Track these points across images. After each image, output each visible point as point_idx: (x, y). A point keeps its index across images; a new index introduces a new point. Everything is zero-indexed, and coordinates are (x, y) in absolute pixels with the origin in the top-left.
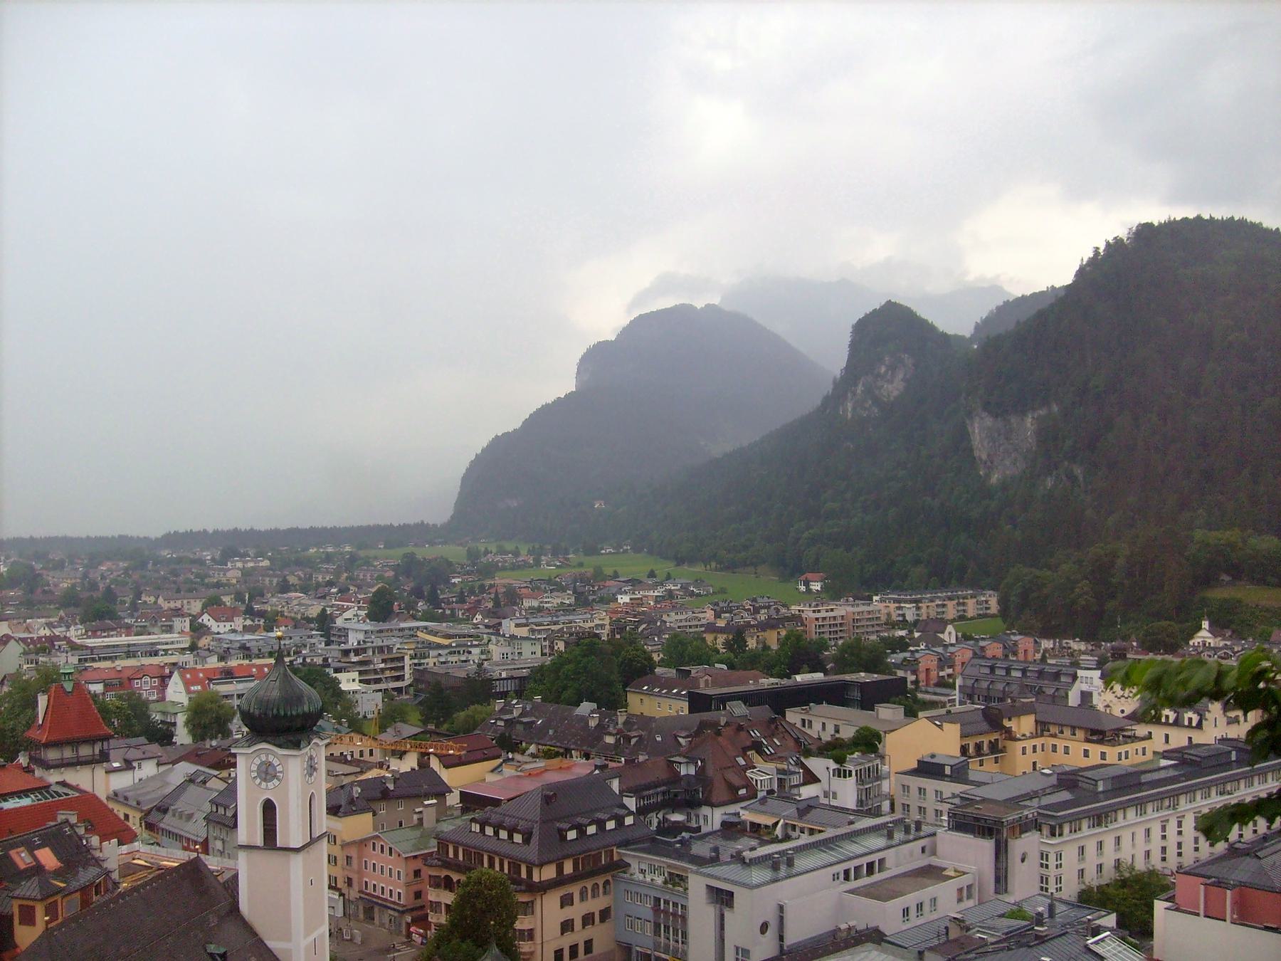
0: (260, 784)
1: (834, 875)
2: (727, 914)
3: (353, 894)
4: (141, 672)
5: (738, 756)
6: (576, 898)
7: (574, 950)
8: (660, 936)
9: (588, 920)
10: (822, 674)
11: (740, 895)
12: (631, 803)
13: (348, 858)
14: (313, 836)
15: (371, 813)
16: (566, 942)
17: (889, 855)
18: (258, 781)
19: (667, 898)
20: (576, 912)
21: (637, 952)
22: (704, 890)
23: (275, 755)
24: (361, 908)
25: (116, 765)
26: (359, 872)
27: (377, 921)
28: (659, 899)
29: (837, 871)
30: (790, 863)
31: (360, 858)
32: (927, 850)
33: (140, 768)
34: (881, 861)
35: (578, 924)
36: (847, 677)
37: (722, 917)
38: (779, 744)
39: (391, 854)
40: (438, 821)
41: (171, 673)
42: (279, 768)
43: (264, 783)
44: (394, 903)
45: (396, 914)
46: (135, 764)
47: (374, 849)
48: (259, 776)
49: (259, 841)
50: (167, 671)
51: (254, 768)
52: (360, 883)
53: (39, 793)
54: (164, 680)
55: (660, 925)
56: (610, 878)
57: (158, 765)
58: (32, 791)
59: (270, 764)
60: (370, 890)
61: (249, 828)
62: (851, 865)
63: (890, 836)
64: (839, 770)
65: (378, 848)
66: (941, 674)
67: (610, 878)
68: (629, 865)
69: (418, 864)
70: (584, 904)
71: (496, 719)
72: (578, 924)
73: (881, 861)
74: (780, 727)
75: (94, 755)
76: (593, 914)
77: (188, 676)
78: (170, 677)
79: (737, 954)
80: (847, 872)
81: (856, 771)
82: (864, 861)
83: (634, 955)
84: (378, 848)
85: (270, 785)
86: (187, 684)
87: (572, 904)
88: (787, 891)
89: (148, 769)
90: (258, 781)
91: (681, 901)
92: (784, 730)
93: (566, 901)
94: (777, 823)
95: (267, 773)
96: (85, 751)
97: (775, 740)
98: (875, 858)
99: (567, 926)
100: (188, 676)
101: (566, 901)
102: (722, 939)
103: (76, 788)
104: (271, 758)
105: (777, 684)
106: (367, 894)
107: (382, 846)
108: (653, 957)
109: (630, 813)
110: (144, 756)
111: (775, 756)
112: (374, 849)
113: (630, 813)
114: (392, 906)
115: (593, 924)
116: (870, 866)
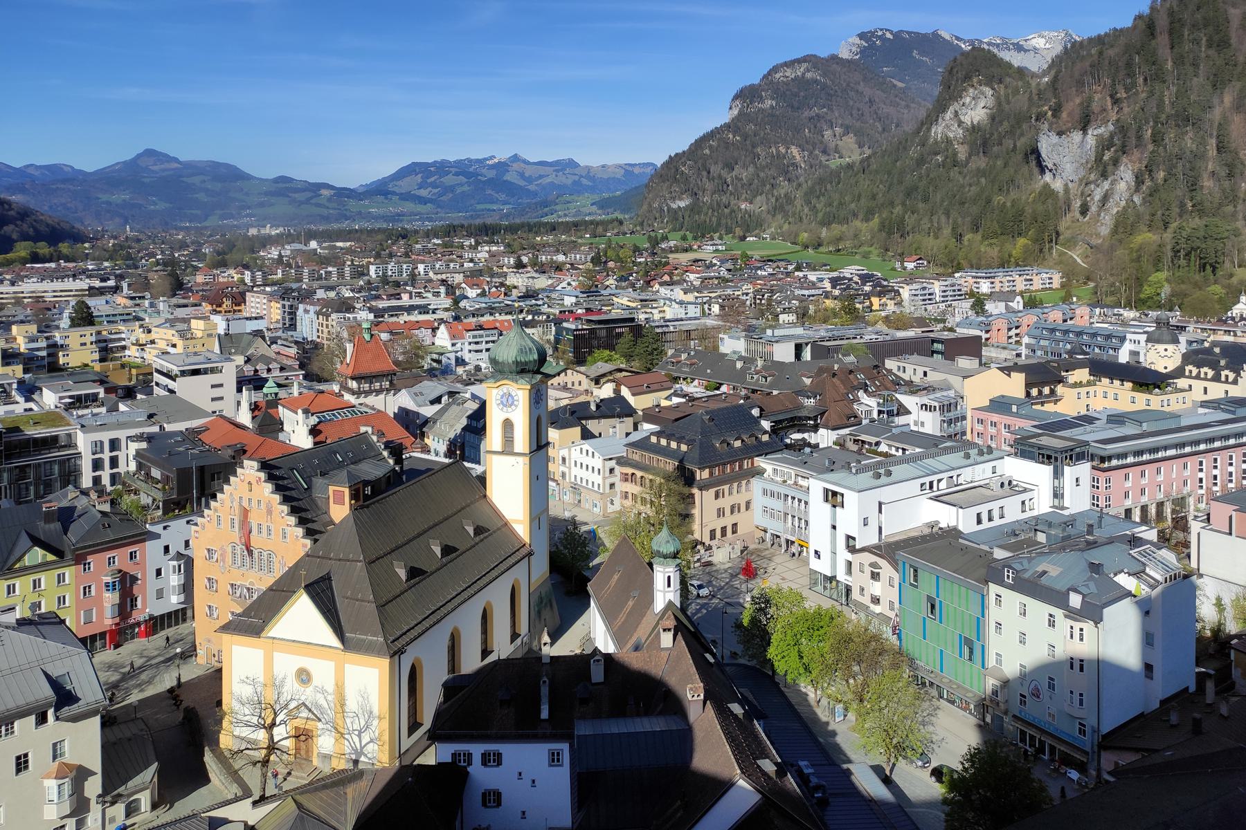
4: (418, 325)
11: (850, 497)
12: (766, 425)
16: (718, 525)
30: (889, 474)
35: (728, 511)
50: (436, 324)
54: (434, 330)
69: (613, 463)
70: (731, 497)
72: (728, 511)
80: (931, 483)
91: (804, 498)
99: (720, 513)
103: (373, 408)
113: (765, 432)
115: (739, 511)
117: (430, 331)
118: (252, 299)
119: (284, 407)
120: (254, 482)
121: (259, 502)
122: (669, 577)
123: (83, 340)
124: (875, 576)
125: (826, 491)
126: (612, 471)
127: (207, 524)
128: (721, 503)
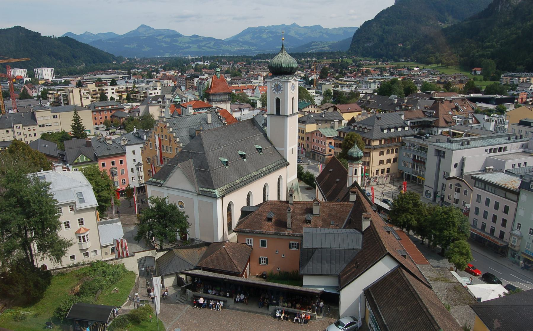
0: (275, 92)
1: (485, 150)
2: (442, 160)
3: (309, 150)
5: (450, 111)
6: (385, 152)
7: (383, 171)
8: (414, 169)
9: (389, 161)
10: (481, 94)
13: (308, 138)
14: (293, 113)
15: (316, 124)
16: (381, 167)
17: (508, 146)
18: (274, 91)
19: (419, 155)
20: (385, 157)
21: (406, 174)
22: (434, 151)
23: (280, 82)
24: (311, 155)
25: (236, 109)
26: (311, 142)
27: (316, 159)
28: (416, 156)
29: (487, 149)
30: (468, 144)
31: (312, 138)
32: (524, 146)
33: (243, 110)
34: (505, 148)
35: (385, 162)
36: (491, 96)
37: (440, 161)
38: (465, 108)
39: (322, 137)
40: (338, 127)
41: (256, 88)
42: (282, 87)
43: (276, 92)
44: (322, 153)
45: (323, 156)
46: (242, 109)
47: (316, 135)
48: (275, 89)
49: (275, 113)
51: (273, 86)
52: (311, 146)
53: (210, 109)
55: (415, 165)
56: (398, 148)
57: (249, 110)
58: (207, 108)
59: (279, 85)
60: (314, 149)
61: (271, 107)
62: (493, 147)
63: (509, 139)
64: (488, 120)
65: (318, 134)
66: (528, 100)
67: (398, 148)
68: (406, 144)
71: (361, 100)
72: (385, 162)
73: (505, 148)
74: (466, 103)
75: (226, 99)
76: (391, 159)
77: (261, 89)
78: (255, 89)
79: (444, 174)
81: (495, 120)
82: (498, 147)
83: (404, 174)
84: (318, 134)
85: (278, 92)
86: (261, 91)
87: (384, 155)
88: (466, 153)
89: (246, 111)
90: (274, 91)
91: (423, 157)
92: (468, 104)
93: (382, 153)
94: (463, 133)
95: (277, 88)
96: (223, 97)
97: (464, 107)
98: (503, 146)
99: (381, 162)
100: (261, 89)
101: (382, 153)
102: (439, 169)
104: (279, 83)
105: (463, 96)
106: (313, 150)
107: (319, 134)
108: (411, 176)
109: (408, 126)
110: (245, 107)
111: (463, 113)
112: (316, 135)
114: (321, 153)
116: (500, 150)
117: (252, 90)
118: (179, 79)
119: (183, 107)
120: (163, 127)
121: (166, 136)
122: (356, 170)
123: (113, 91)
124: (458, 191)
125: (436, 149)
126: (330, 143)
127: (146, 147)
128: (382, 158)
